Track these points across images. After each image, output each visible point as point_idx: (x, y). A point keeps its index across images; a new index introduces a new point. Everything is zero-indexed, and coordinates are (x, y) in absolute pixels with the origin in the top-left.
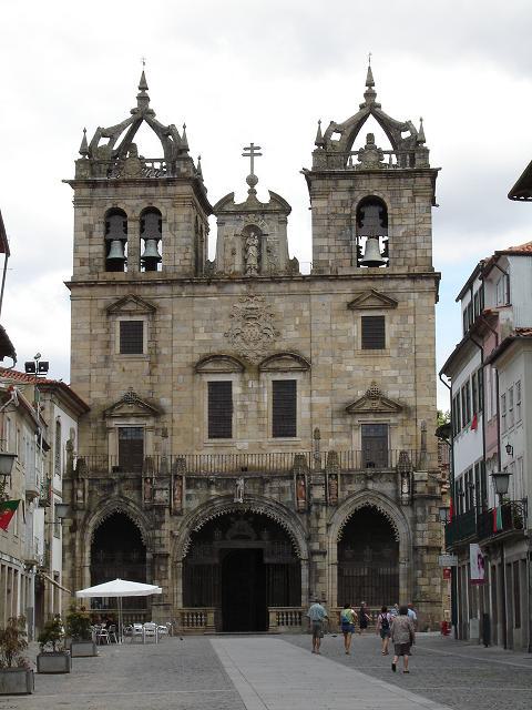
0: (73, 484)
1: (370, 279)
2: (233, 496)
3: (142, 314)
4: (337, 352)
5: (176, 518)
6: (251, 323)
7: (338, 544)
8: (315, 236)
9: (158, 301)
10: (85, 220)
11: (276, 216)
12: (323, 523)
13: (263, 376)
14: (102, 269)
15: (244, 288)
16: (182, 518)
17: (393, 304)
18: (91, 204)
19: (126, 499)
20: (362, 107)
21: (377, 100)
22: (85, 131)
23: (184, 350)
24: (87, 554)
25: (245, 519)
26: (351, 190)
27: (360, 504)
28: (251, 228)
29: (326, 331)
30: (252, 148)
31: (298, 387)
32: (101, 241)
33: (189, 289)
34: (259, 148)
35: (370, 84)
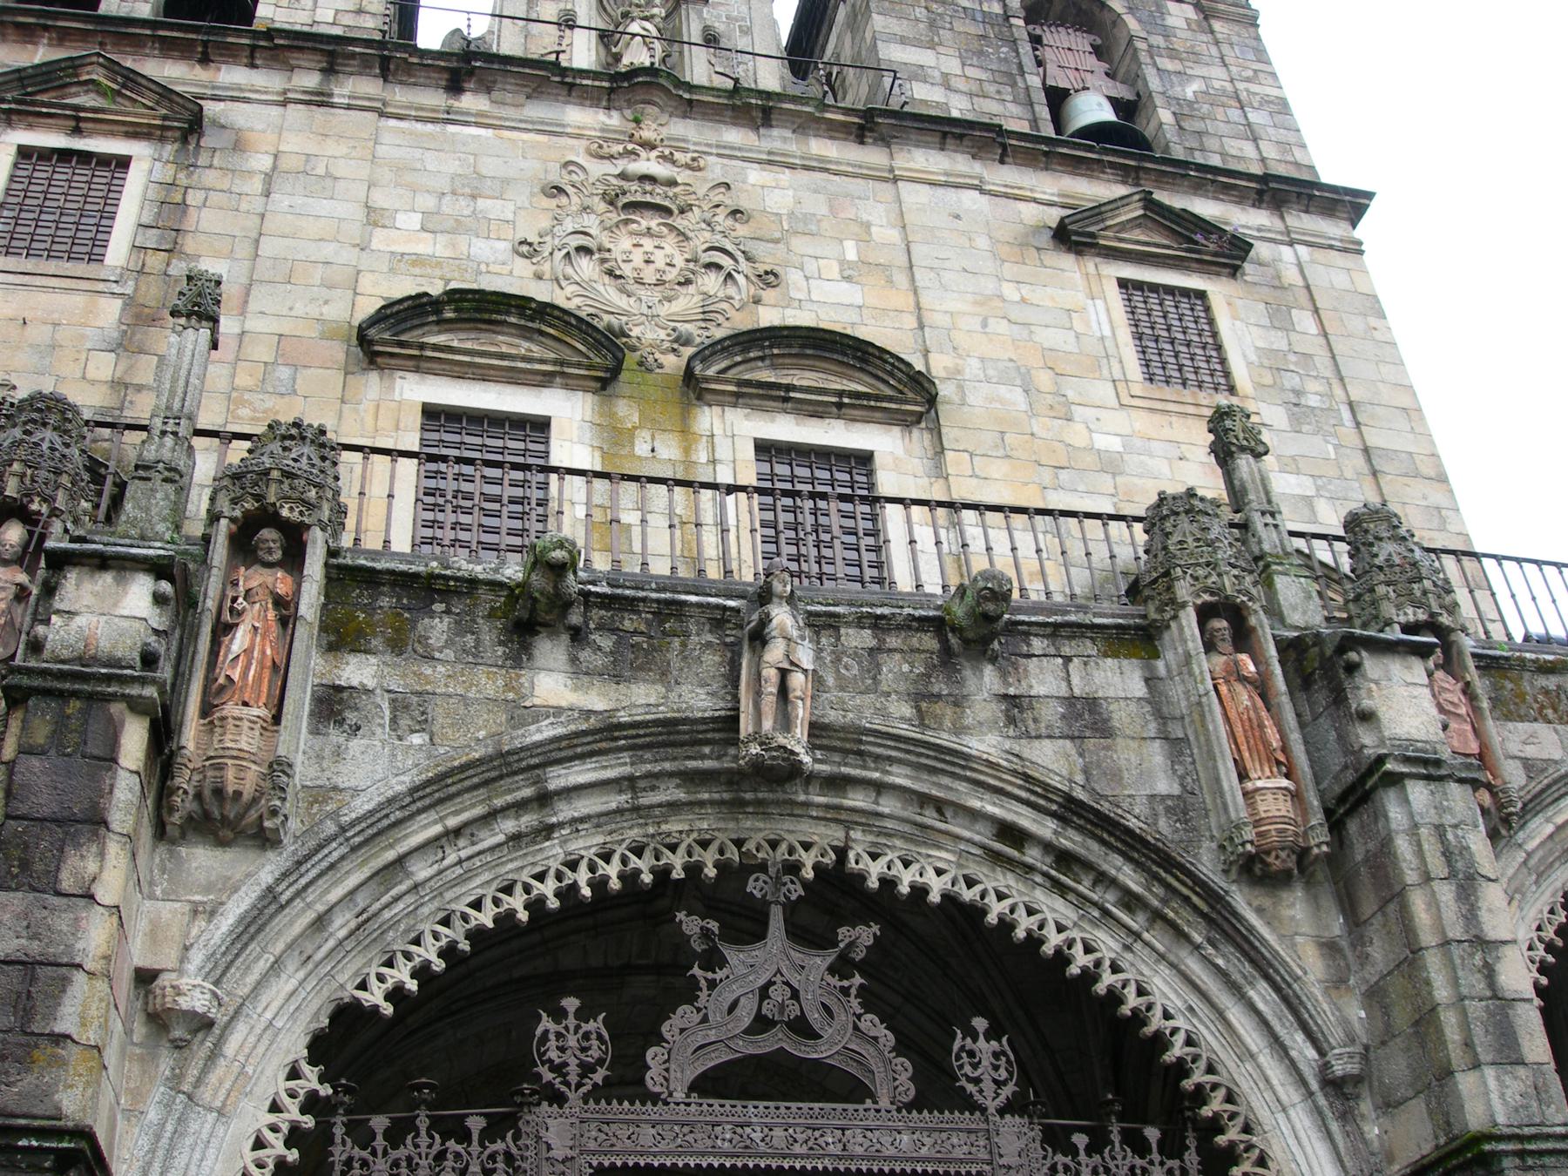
3: (135, 132)
4: (1044, 379)
5: (202, 859)
6: (653, 222)
9: (222, 105)
13: (708, 419)
15: (614, 120)
16: (268, 868)
23: (318, 274)
25: (806, 934)
29: (982, 301)
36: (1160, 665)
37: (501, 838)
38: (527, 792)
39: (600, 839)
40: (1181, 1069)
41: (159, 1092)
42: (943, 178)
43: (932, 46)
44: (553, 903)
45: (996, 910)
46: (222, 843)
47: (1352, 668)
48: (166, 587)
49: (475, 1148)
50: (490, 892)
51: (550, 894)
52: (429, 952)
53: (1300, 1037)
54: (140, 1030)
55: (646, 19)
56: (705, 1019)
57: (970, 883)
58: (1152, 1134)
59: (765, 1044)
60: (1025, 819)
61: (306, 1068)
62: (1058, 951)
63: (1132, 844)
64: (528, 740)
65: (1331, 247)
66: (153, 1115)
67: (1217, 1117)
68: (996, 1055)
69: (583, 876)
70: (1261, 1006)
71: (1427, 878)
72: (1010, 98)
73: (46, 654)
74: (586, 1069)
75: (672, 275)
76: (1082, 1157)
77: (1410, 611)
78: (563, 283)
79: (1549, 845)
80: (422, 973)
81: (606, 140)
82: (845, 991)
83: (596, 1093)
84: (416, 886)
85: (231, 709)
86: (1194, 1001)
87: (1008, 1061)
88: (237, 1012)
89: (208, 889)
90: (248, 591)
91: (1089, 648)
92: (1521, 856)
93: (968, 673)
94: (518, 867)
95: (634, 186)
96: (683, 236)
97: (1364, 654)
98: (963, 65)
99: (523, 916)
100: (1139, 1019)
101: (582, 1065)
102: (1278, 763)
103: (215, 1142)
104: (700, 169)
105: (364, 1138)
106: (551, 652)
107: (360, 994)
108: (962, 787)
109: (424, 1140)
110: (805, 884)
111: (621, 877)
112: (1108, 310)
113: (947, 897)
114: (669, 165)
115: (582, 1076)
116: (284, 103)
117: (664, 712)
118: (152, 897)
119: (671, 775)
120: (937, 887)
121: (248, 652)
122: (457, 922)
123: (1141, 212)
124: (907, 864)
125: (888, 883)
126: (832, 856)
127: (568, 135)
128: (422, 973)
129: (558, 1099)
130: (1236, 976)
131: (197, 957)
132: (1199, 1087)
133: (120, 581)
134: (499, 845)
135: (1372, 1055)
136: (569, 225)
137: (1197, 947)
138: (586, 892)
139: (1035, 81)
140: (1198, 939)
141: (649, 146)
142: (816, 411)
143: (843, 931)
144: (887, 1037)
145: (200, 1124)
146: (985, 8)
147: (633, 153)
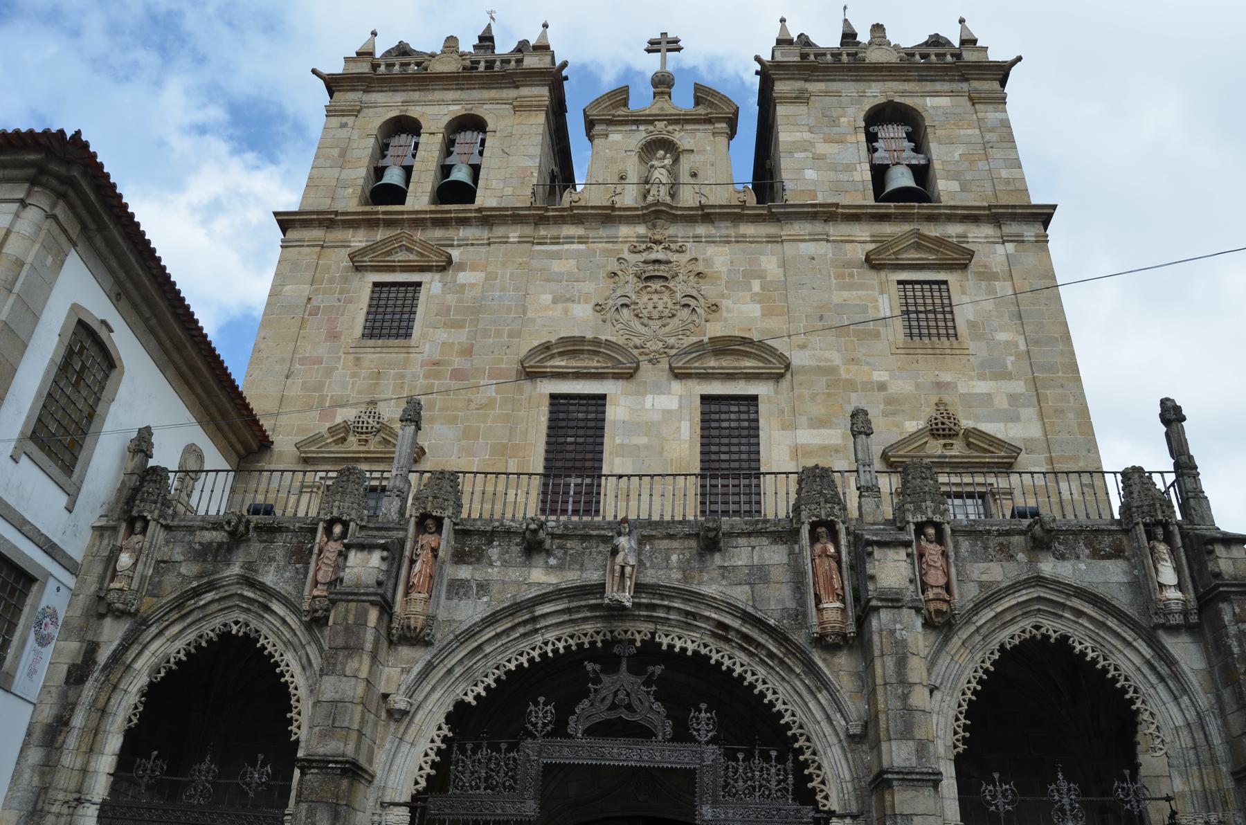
0: (116, 539)
2: (600, 588)
5: (405, 651)
6: (656, 285)
7: (959, 761)
12: (917, 669)
15: (641, 230)
17: (960, 259)
18: (359, 111)
19: (263, 588)
24: (105, 763)
27: (1014, 629)
31: (762, 407)
32: (366, 161)
34: (676, 41)
36: (796, 547)
37: (518, 635)
38: (527, 617)
39: (557, 633)
40: (788, 726)
41: (390, 737)
44: (538, 659)
45: (715, 657)
46: (412, 645)
47: (870, 554)
48: (385, 554)
49: (503, 756)
50: (514, 656)
51: (536, 656)
52: (490, 681)
53: (839, 715)
54: (384, 715)
55: (662, 167)
56: (592, 705)
57: (706, 646)
58: (773, 754)
59: (613, 715)
60: (728, 620)
61: (444, 726)
62: (740, 675)
63: (772, 631)
64: (526, 597)
66: (387, 746)
67: (801, 748)
68: (709, 719)
69: (549, 648)
70: (823, 701)
71: (882, 655)
73: (344, 584)
74: (545, 725)
75: (667, 312)
76: (741, 763)
77: (919, 516)
78: (615, 323)
79: (994, 621)
80: (487, 688)
81: (637, 242)
82: (648, 693)
83: (548, 735)
84: (485, 656)
85: (414, 595)
86: (796, 697)
87: (714, 722)
88: (419, 707)
89: (407, 663)
90: (422, 546)
91: (765, 541)
92: (973, 628)
93: (708, 557)
94: (524, 645)
95: (651, 268)
96: (673, 292)
97: (875, 548)
99: (526, 665)
100: (772, 704)
101: (544, 723)
102: (838, 595)
103: (410, 755)
104: (683, 252)
105: (463, 752)
106: (539, 559)
107: (465, 697)
108: (703, 607)
109: (485, 752)
110: (636, 648)
111: (565, 648)
112: (890, 300)
113: (696, 653)
114: (668, 252)
115: (543, 728)
116: (489, 244)
117: (578, 583)
118: (388, 666)
119: (585, 606)
120: (691, 647)
121: (420, 571)
122: (502, 668)
124: (680, 638)
125: (671, 647)
126: (649, 636)
128: (487, 688)
129: (534, 737)
130: (814, 689)
131: (403, 688)
132: (794, 735)
133: (370, 552)
134: (517, 638)
135: (869, 725)
136: (619, 293)
137: (798, 675)
138: (550, 654)
139: (867, 167)
140: (798, 671)
142: (729, 377)
143: (651, 668)
144: (662, 710)
145: (405, 748)
147: (648, 249)
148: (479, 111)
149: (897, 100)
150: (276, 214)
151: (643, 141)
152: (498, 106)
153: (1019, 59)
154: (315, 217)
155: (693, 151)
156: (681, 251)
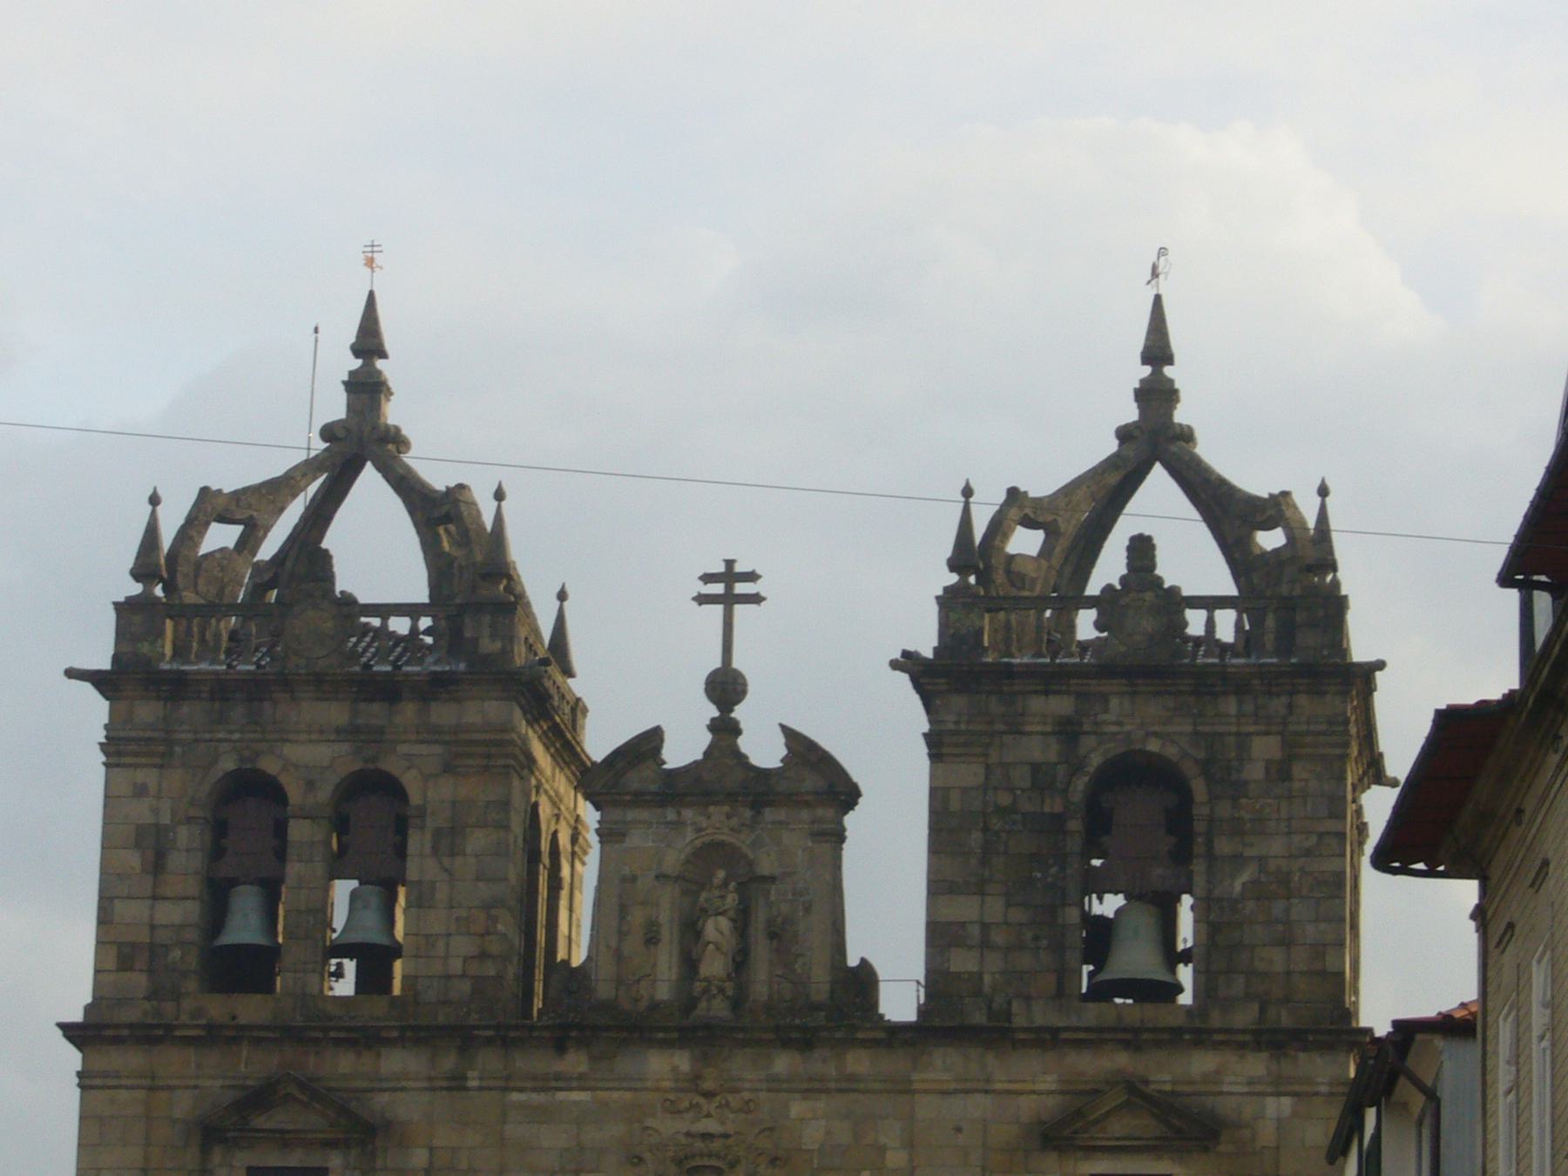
1: (1126, 1045)
8: (938, 888)
9: (386, 1097)
10: (141, 811)
11: (805, 814)
14: (192, 985)
15: (682, 1061)
20: (1124, 434)
21: (1181, 416)
22: (154, 500)
26: (1068, 731)
28: (710, 854)
30: (730, 575)
32: (192, 886)
33: (488, 1061)
34: (751, 577)
35: (1157, 351)
42: (953, 1086)
43: (980, 889)
55: (720, 914)
65: (1317, 1094)
72: (1045, 943)
81: (677, 1090)
98: (1008, 905)
123: (1125, 1097)
127: (646, 1089)
141: (709, 1095)
146: (1047, 809)
148: (392, 765)
149: (1153, 746)
150: (62, 1026)
151: (689, 850)
152: (423, 749)
153: (1380, 665)
154: (125, 1032)
155: (772, 879)
156: (746, 1108)
